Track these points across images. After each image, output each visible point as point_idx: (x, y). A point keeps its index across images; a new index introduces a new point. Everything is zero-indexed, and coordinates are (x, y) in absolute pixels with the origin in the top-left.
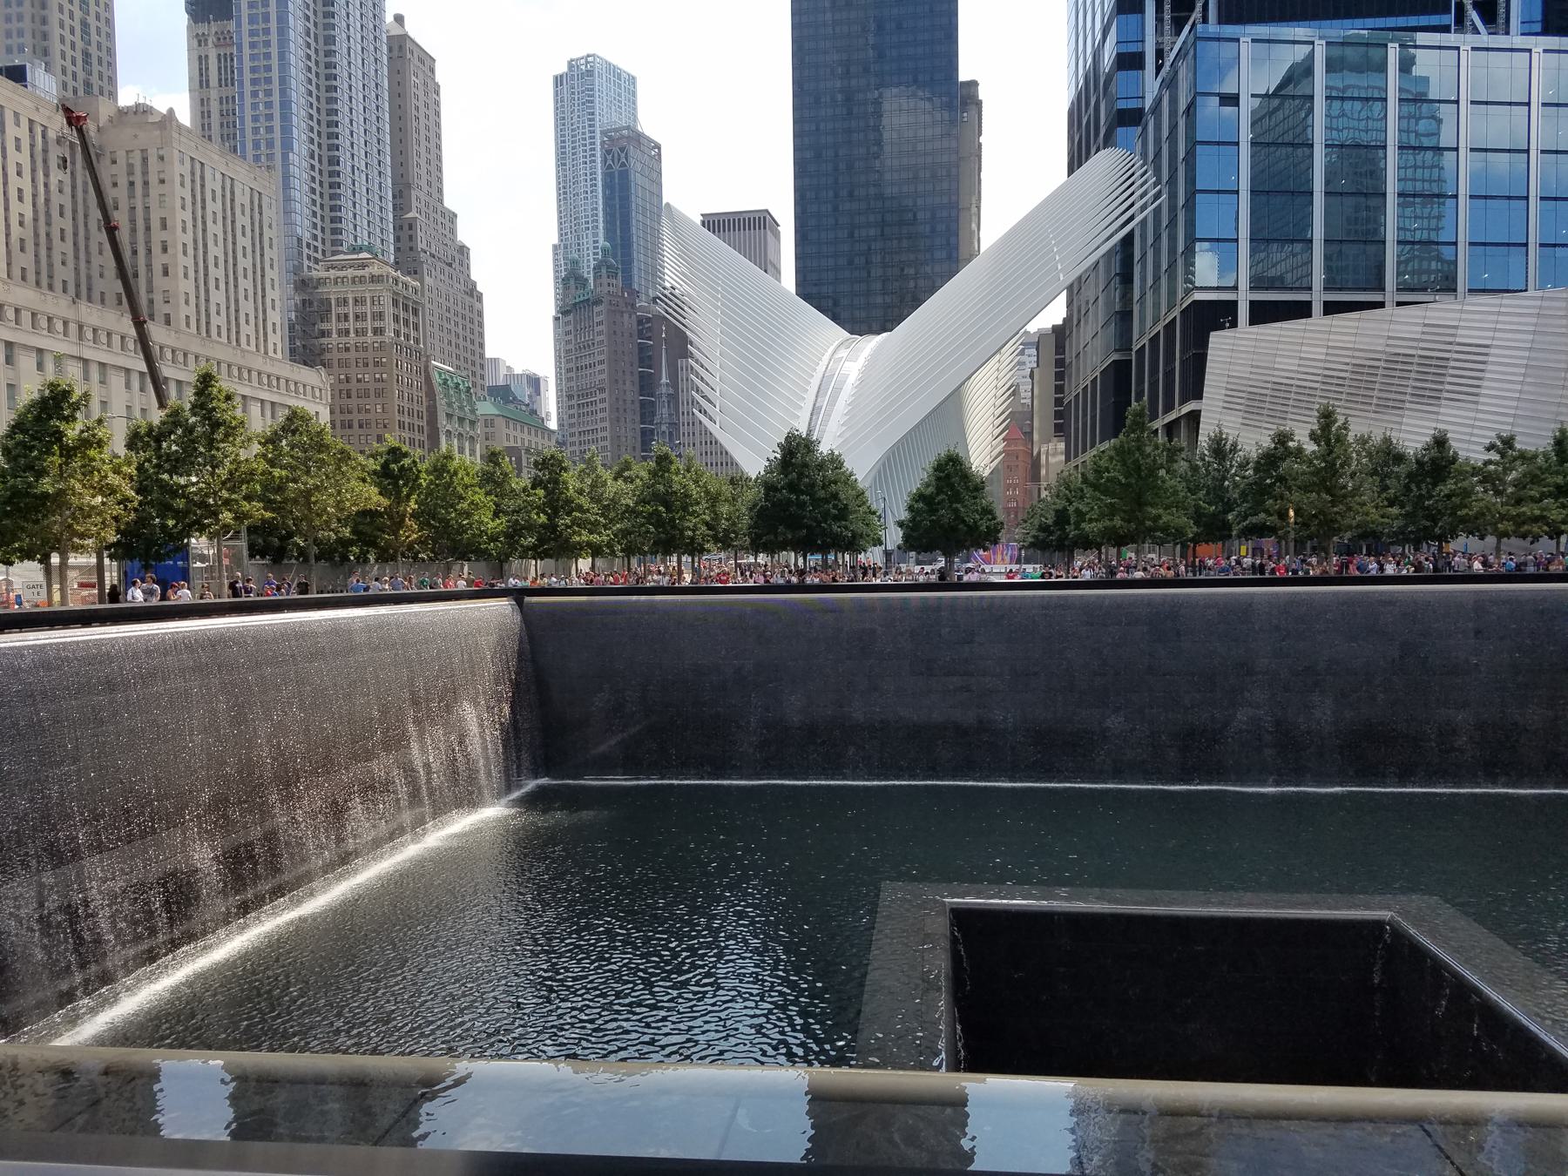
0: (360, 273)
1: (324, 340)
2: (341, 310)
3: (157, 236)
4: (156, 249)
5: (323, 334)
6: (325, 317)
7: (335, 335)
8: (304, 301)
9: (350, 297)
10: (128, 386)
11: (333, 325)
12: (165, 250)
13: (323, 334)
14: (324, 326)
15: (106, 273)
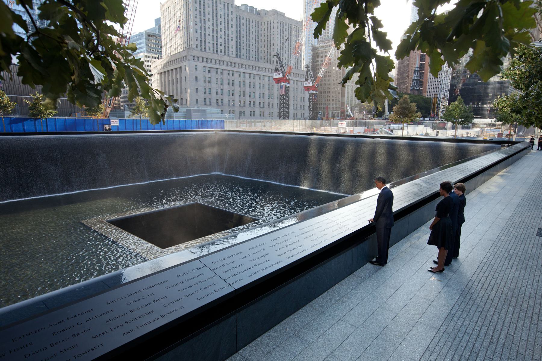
0: (326, 44)
1: (317, 63)
2: (322, 55)
3: (272, 42)
4: (272, 45)
5: (318, 61)
6: (318, 57)
7: (320, 62)
8: (314, 53)
9: (324, 51)
10: (260, 78)
11: (320, 59)
12: (273, 45)
13: (318, 61)
14: (317, 59)
15: (262, 52)
